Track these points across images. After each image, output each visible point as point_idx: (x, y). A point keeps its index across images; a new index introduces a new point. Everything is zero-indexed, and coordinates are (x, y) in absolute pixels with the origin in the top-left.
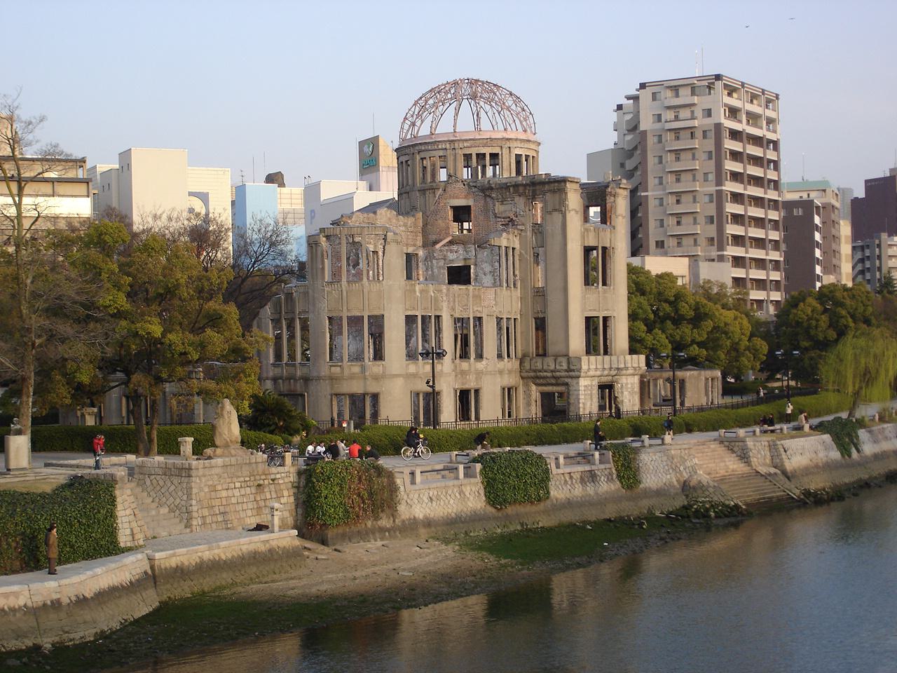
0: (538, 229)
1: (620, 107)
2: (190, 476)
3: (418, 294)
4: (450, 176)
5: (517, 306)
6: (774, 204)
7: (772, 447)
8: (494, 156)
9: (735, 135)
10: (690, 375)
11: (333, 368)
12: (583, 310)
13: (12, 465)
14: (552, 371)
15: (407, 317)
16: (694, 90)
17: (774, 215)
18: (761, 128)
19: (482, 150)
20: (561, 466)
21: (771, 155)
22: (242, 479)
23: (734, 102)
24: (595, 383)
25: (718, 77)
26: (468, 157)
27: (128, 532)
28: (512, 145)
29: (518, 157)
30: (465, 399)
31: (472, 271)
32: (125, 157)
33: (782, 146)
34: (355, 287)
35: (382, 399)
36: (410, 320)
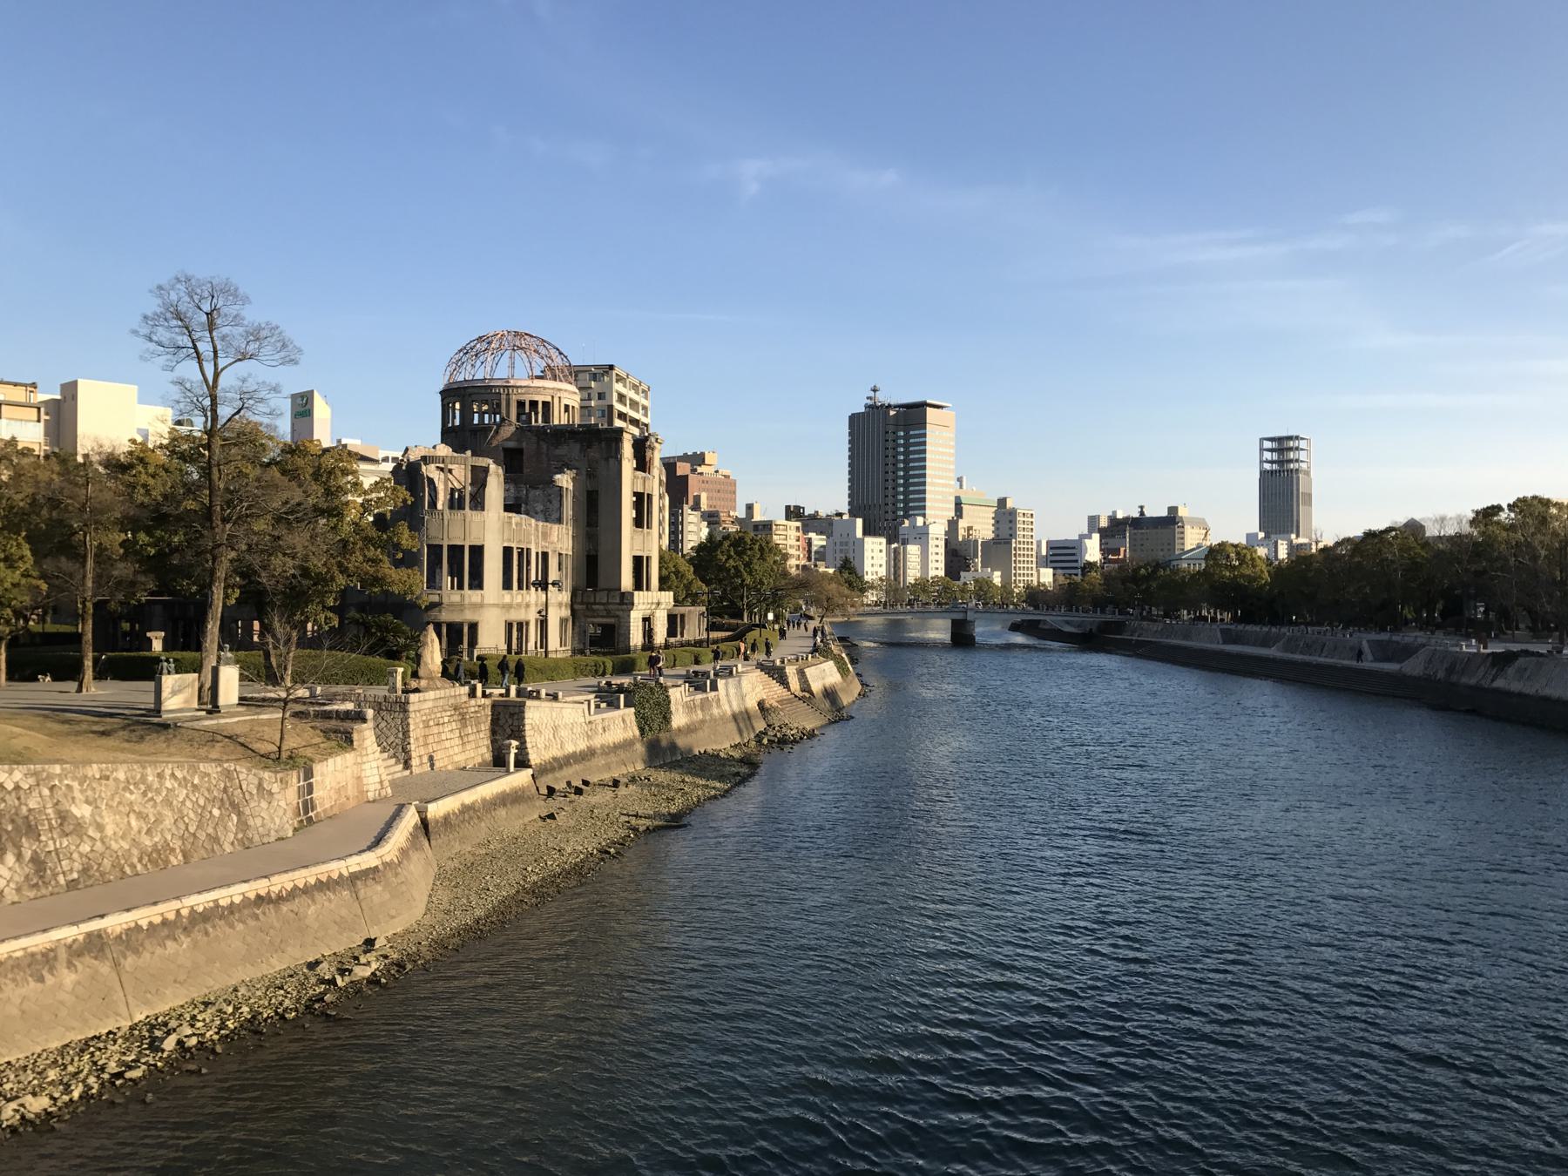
0: (591, 475)
2: (406, 711)
3: (514, 526)
4: (503, 420)
7: (801, 674)
8: (546, 405)
9: (622, 416)
10: (689, 611)
11: (431, 596)
12: (632, 549)
14: (603, 604)
15: (504, 548)
16: (594, 377)
18: (638, 412)
19: (536, 398)
22: (449, 713)
23: (624, 391)
25: (611, 367)
26: (521, 404)
27: (377, 779)
28: (562, 395)
29: (567, 407)
34: (459, 515)
36: (507, 552)
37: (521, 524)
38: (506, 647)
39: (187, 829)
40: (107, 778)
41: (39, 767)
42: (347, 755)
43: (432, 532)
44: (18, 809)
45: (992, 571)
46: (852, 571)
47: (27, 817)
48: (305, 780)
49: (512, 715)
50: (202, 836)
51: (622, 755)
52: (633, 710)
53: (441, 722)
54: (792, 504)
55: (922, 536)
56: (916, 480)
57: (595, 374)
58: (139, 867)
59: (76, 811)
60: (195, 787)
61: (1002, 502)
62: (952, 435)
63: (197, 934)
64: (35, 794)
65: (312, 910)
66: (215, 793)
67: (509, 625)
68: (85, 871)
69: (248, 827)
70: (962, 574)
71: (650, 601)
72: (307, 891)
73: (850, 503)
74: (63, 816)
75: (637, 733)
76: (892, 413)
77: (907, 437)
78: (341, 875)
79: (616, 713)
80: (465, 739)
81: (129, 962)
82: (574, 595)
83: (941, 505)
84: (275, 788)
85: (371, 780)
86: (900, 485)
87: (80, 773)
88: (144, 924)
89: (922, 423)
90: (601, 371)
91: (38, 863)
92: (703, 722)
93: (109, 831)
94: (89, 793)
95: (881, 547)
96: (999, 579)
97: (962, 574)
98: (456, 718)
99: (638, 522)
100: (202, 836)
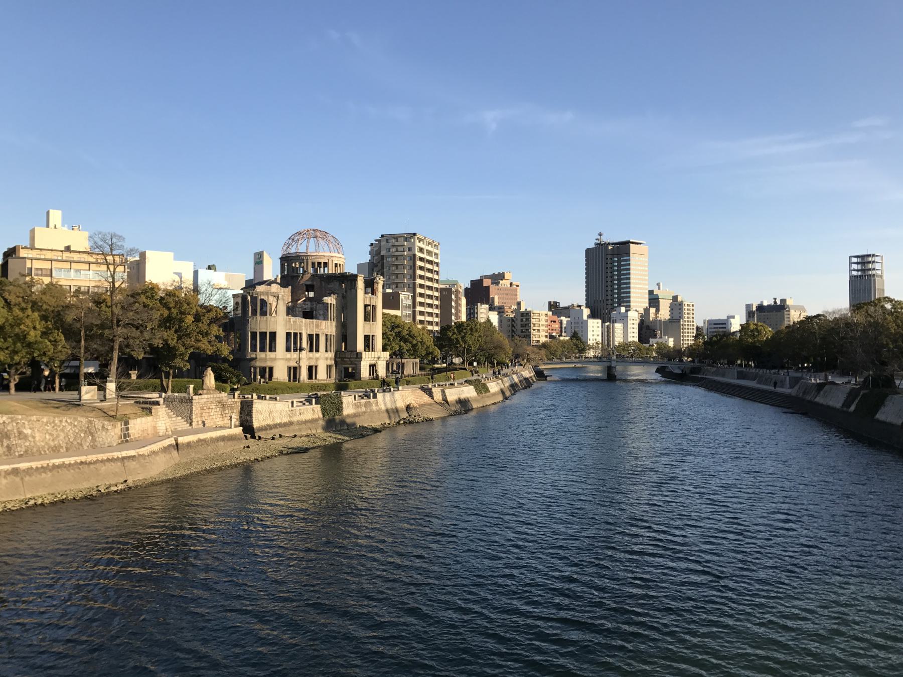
0: (344, 297)
1: (372, 244)
2: (192, 403)
3: (292, 323)
5: (334, 329)
6: (437, 289)
7: (443, 392)
9: (421, 259)
10: (407, 362)
12: (364, 332)
13: (108, 396)
17: (436, 294)
18: (432, 256)
19: (320, 261)
20: (357, 399)
21: (436, 268)
23: (421, 245)
24: (368, 364)
25: (415, 234)
27: (165, 428)
29: (336, 265)
30: (312, 370)
31: (314, 313)
32: (143, 255)
33: (440, 265)
34: (264, 318)
35: (274, 369)
36: (288, 334)
37: (296, 322)
38: (287, 378)
39: (69, 440)
40: (39, 421)
41: (13, 416)
42: (148, 418)
43: (252, 327)
44: (3, 429)
45: (668, 338)
46: (578, 339)
47: (6, 432)
48: (125, 425)
49: (248, 406)
50: (75, 443)
51: (309, 425)
52: (319, 406)
53: (211, 407)
54: (552, 300)
55: (624, 319)
56: (624, 286)
57: (406, 238)
58: (47, 452)
59: (25, 431)
60: (75, 426)
61: (675, 298)
62: (647, 260)
63: (55, 472)
64: (11, 425)
65: (103, 469)
66: (83, 428)
67: (290, 368)
68: (26, 451)
69: (96, 441)
70: (651, 340)
71: (373, 356)
72: (102, 461)
73: (586, 300)
74: (20, 433)
75: (321, 416)
76: (610, 248)
77: (619, 261)
78: (118, 457)
79: (311, 406)
80: (224, 415)
81: (27, 478)
82: (336, 354)
83: (640, 300)
84: (109, 428)
85: (161, 428)
86: (615, 289)
87: (29, 418)
88: (34, 467)
89: (628, 254)
90: (409, 236)
91: (9, 448)
92: (365, 412)
93: (37, 439)
94: (31, 426)
95: (598, 325)
96: (673, 343)
97: (651, 340)
98: (219, 406)
99: (367, 319)
100: (75, 443)
